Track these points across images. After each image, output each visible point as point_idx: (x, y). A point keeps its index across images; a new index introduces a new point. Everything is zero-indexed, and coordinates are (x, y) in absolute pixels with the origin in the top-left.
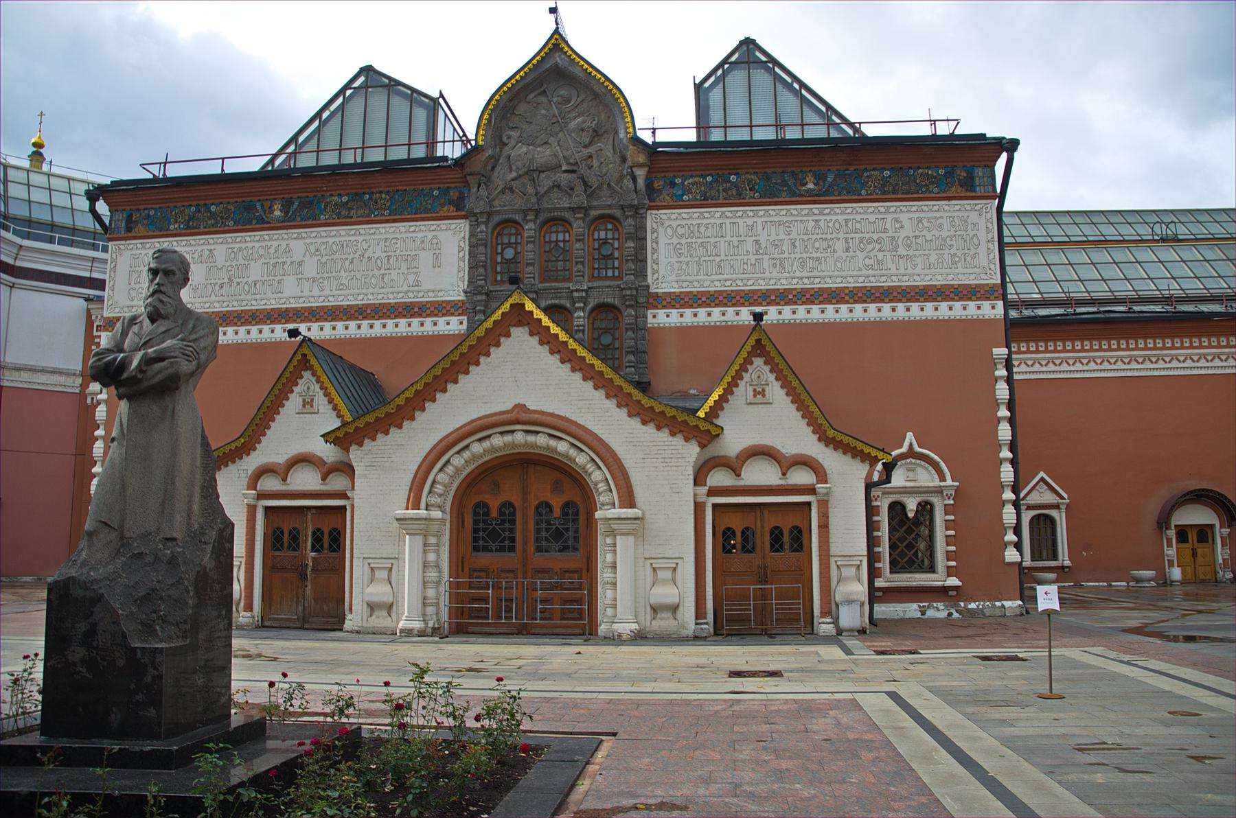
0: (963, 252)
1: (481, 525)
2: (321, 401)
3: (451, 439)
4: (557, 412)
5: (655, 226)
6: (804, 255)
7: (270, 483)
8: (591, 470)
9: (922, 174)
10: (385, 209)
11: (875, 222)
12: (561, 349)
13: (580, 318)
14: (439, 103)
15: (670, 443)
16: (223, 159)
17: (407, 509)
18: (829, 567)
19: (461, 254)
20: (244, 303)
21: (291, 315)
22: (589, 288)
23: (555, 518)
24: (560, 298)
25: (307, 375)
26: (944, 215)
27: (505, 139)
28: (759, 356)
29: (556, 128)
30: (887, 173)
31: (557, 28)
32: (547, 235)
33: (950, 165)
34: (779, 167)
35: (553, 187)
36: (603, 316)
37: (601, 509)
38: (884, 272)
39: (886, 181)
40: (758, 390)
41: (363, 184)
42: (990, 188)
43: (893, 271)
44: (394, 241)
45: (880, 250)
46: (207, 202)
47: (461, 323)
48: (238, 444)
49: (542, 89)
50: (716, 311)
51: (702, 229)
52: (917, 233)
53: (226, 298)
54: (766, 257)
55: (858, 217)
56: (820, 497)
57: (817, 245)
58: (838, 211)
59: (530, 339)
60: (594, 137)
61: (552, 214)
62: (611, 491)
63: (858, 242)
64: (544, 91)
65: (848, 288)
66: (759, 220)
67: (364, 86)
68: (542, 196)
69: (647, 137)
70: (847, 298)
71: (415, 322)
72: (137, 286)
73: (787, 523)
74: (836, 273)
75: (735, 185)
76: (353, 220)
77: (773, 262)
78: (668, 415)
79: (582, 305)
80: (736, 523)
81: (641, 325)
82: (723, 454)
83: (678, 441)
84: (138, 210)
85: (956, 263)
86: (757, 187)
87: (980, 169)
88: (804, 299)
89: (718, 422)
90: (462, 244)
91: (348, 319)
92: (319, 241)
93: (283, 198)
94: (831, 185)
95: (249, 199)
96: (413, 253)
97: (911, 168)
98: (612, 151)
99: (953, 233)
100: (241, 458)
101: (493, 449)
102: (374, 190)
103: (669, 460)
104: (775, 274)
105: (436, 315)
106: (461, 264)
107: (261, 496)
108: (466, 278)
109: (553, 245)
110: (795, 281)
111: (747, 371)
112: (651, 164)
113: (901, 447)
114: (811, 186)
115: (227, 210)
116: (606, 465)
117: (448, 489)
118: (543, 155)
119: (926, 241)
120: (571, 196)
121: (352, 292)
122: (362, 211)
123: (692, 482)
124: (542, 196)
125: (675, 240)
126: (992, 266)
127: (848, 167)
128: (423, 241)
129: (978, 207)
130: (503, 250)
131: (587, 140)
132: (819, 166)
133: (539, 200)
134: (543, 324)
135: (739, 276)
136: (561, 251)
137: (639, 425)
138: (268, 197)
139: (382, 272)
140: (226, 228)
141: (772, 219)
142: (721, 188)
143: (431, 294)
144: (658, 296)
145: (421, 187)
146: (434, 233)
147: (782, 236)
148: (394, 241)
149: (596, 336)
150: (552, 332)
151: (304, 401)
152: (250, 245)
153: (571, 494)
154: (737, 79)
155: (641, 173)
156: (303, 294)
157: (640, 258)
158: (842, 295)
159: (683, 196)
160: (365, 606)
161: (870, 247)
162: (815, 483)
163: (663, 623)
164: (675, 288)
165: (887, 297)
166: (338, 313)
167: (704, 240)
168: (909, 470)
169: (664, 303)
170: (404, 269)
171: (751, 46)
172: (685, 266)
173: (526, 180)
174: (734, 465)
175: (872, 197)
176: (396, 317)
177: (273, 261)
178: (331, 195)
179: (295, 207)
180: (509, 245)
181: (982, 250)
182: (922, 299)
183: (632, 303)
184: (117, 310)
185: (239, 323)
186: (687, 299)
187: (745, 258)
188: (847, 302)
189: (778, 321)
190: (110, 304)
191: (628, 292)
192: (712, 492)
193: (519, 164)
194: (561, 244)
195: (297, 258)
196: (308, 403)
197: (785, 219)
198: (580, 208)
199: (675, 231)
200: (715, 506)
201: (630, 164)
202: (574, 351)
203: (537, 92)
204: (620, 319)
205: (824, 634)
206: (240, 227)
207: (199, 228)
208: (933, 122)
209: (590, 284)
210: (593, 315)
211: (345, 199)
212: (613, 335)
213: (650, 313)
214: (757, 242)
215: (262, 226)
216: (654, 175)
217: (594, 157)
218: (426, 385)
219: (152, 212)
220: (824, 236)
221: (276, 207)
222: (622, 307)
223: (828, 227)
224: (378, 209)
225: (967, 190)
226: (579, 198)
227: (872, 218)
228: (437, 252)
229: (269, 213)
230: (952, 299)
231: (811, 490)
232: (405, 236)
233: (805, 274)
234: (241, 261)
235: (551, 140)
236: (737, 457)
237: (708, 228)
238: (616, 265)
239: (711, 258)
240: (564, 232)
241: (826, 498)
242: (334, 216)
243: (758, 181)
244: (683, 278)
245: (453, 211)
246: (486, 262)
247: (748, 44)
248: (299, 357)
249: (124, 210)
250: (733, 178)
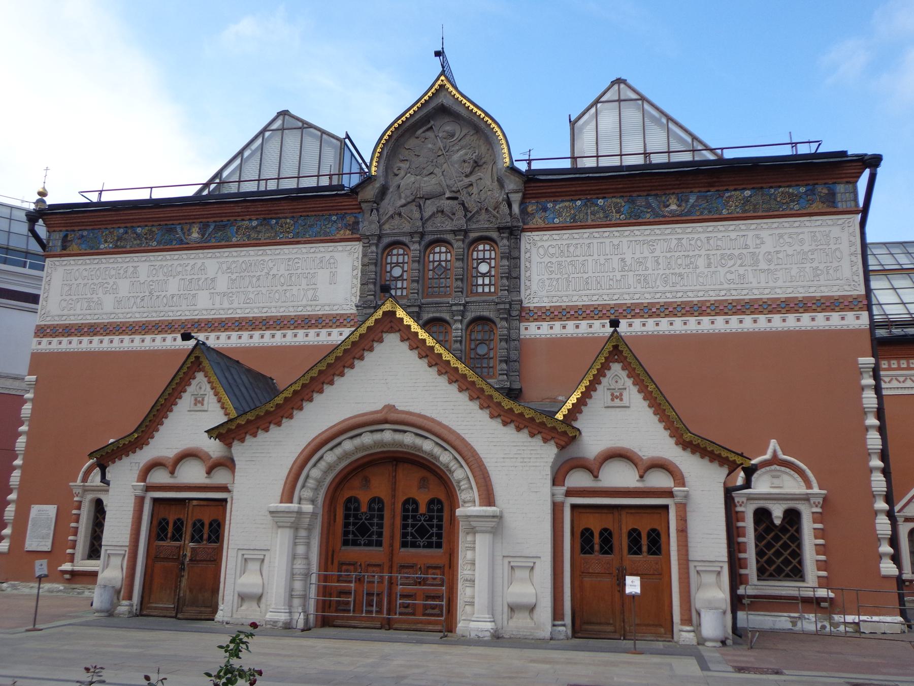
0: (826, 265)
1: (352, 520)
2: (211, 401)
3: (324, 437)
4: (423, 413)
5: (528, 246)
6: (667, 272)
7: (159, 477)
8: (454, 468)
9: (782, 193)
10: (289, 233)
11: (736, 239)
12: (428, 353)
13: (457, 328)
14: (345, 144)
15: (529, 444)
16: (151, 188)
17: (281, 502)
18: (688, 573)
19: (355, 273)
20: (162, 314)
21: (203, 325)
22: (467, 303)
23: (421, 515)
24: (440, 312)
25: (200, 376)
26: (806, 230)
27: (396, 171)
28: (617, 361)
29: (441, 160)
30: (747, 193)
31: (443, 71)
32: (431, 256)
33: (811, 182)
34: (644, 191)
35: (438, 212)
36: (480, 328)
37: (463, 506)
38: (745, 285)
39: (747, 201)
40: (615, 394)
41: (271, 210)
42: (853, 203)
43: (755, 284)
44: (296, 260)
45: (741, 265)
46: (134, 225)
48: (132, 439)
49: (429, 126)
50: (584, 324)
51: (572, 249)
52: (778, 249)
53: (146, 309)
54: (631, 274)
55: (720, 235)
56: (677, 500)
57: (679, 262)
58: (700, 229)
59: (402, 343)
60: (475, 167)
61: (436, 236)
62: (472, 488)
63: (719, 258)
64: (431, 128)
65: (709, 301)
66: (625, 240)
67: (282, 129)
68: (427, 220)
69: (523, 167)
70: (708, 311)
71: (312, 332)
72: (68, 298)
73: (644, 525)
74: (698, 287)
75: (602, 208)
76: (260, 242)
77: (638, 278)
78: (527, 416)
79: (460, 318)
80: (595, 524)
81: (514, 336)
82: (581, 455)
83: (537, 441)
84: (74, 231)
85: (818, 275)
86: (622, 209)
87: (842, 186)
88: (667, 312)
89: (576, 424)
90: (356, 264)
91: (253, 329)
92: (231, 260)
93: (201, 222)
94: (693, 206)
95: (171, 222)
96: (312, 272)
97: (771, 187)
98: (490, 180)
99: (814, 247)
101: (364, 447)
102: (280, 216)
103: (528, 460)
104: (639, 289)
105: (331, 327)
106: (355, 281)
107: (149, 488)
108: (358, 294)
109: (436, 264)
110: (658, 295)
111: (605, 376)
112: (525, 190)
113: (765, 454)
114: (673, 207)
115: (151, 232)
116: (468, 464)
117: (321, 484)
118: (429, 184)
119: (787, 255)
120: (453, 220)
121: (257, 305)
122: (269, 235)
123: (549, 482)
124: (427, 220)
125: (547, 259)
126: (856, 278)
127: (710, 189)
128: (322, 261)
129: (840, 222)
130: (392, 268)
131: (468, 170)
132: (681, 188)
133: (423, 224)
134: (412, 330)
135: (605, 291)
136: (443, 269)
137: (500, 426)
138: (188, 221)
139: (285, 287)
140: (150, 248)
141: (637, 238)
142: (589, 211)
143: (327, 308)
144: (530, 310)
145: (321, 213)
146: (332, 254)
147: (646, 254)
148: (296, 260)
149: (473, 346)
150: (420, 337)
151: (196, 400)
152: (169, 263)
155: (516, 198)
156: (215, 307)
157: (514, 275)
158: (704, 308)
159: (555, 218)
160: (236, 596)
161: (731, 263)
162: (673, 486)
163: (520, 624)
164: (546, 303)
165: (748, 309)
166: (244, 324)
167: (573, 258)
168: (773, 477)
169: (536, 317)
170: (304, 286)
171: (622, 86)
172: (555, 283)
173: (413, 207)
174: (592, 468)
175: (733, 216)
176: (295, 328)
177: (189, 277)
178: (243, 220)
179: (211, 230)
180: (397, 264)
181: (846, 265)
182: (784, 311)
183: (506, 316)
184: (48, 319)
185: (156, 332)
186: (556, 313)
187: (611, 275)
188: (709, 315)
189: (642, 332)
190: (43, 313)
191: (502, 306)
192: (570, 493)
193: (408, 192)
194: (443, 264)
195: (211, 274)
196: (199, 402)
197: (649, 238)
198: (460, 230)
199: (546, 251)
200: (574, 507)
201: (507, 191)
202: (440, 355)
203: (424, 128)
204: (495, 331)
205: (683, 643)
206: (162, 247)
207: (125, 247)
208: (794, 145)
209: (468, 299)
210: (471, 327)
211: (254, 223)
212: (488, 346)
213: (523, 325)
214: (623, 260)
215: (181, 246)
216: (528, 201)
217: (475, 185)
218: (304, 386)
219: (85, 233)
220: (686, 253)
221: (194, 230)
222: (497, 320)
223: (690, 244)
224: (282, 232)
225: (828, 206)
226: (460, 222)
227: (733, 235)
228: (333, 270)
229: (188, 235)
230: (815, 311)
231: (669, 494)
232: (305, 256)
233: (668, 288)
234: (161, 277)
235: (437, 171)
236: (594, 459)
237: (577, 248)
238: (493, 282)
239: (579, 275)
240: (446, 252)
241: (684, 501)
242: (245, 238)
243: (623, 204)
244: (553, 293)
245: (348, 235)
246: (376, 279)
248: (192, 359)
249: (61, 231)
250: (600, 202)
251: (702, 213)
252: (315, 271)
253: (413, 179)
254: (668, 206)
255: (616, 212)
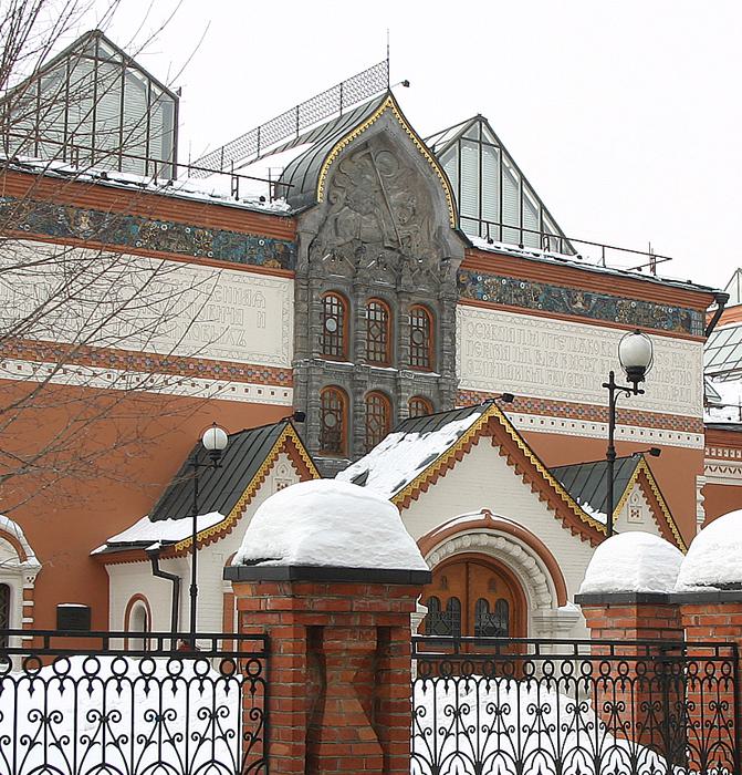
30: (634, 304)
47: (286, 395)
90: (286, 306)
94: (594, 308)
105: (262, 383)
114: (580, 305)
118: (369, 227)
153: (502, 591)
154: (469, 153)
211: (164, 227)
217: (413, 237)
229: (75, 225)
247: (480, 119)
251: (601, 317)
252: (242, 307)
253: (352, 215)
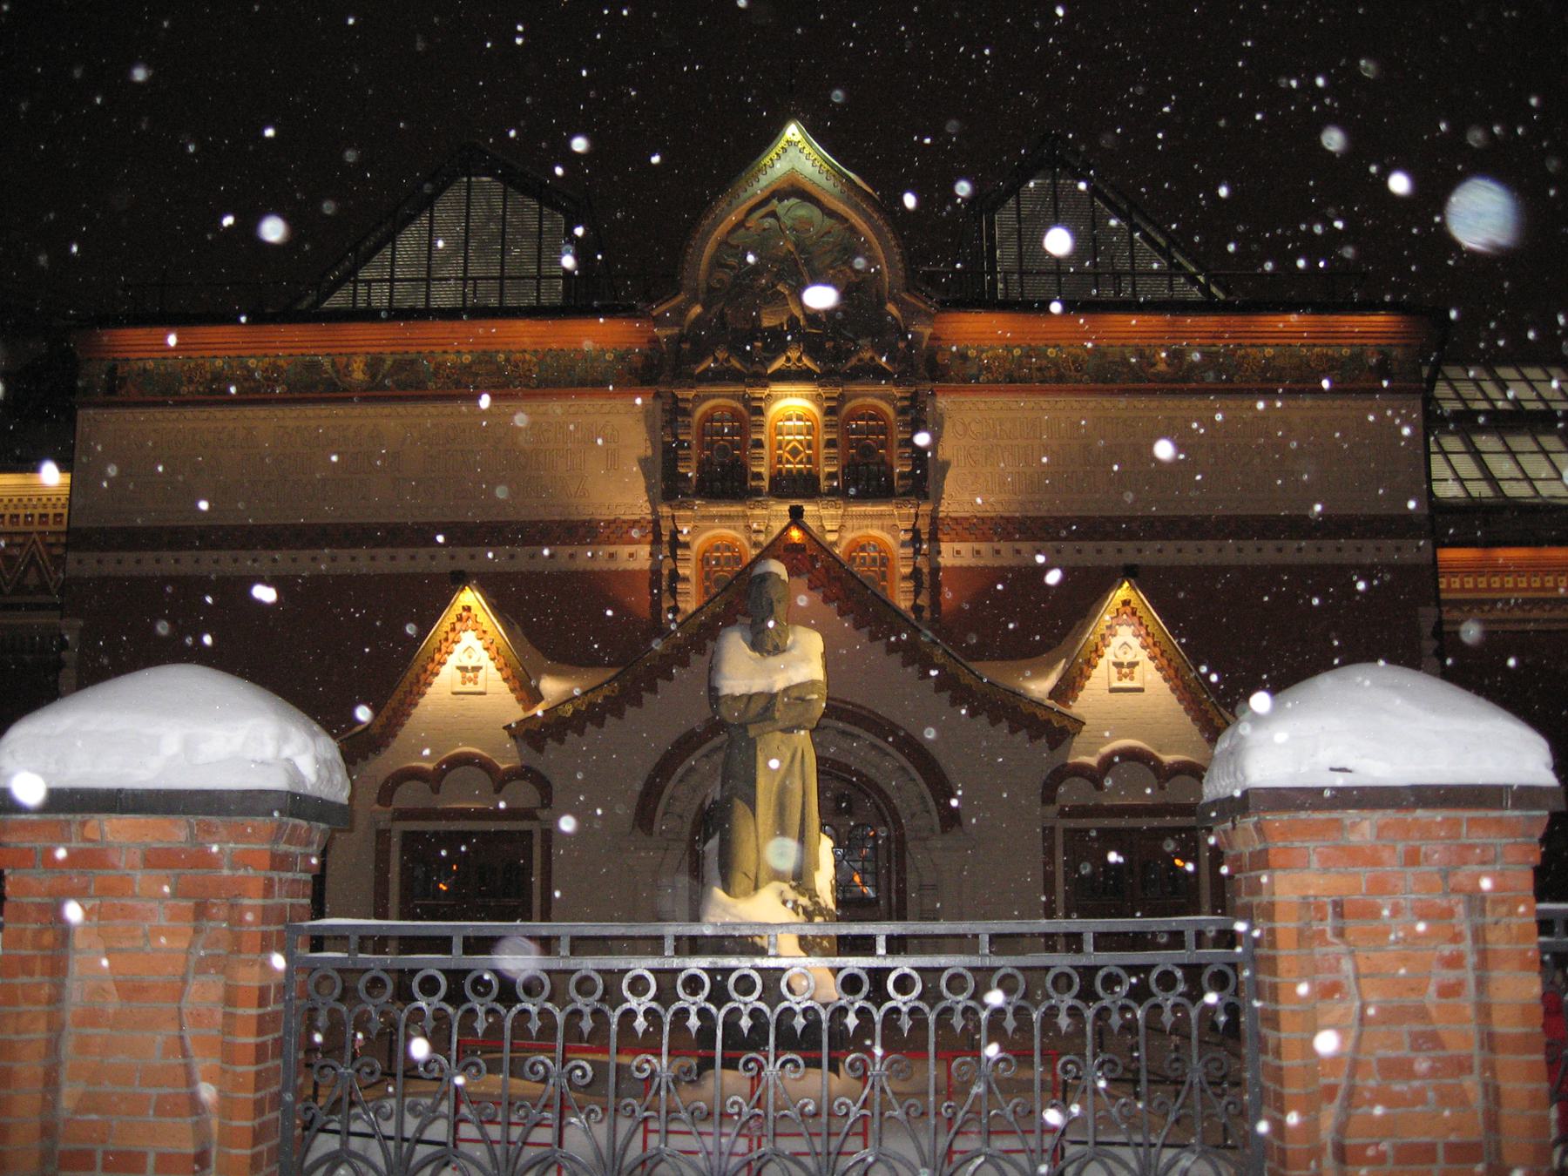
7: (409, 796)
100: (366, 758)
138: (343, 350)
178: (445, 352)
192: (1062, 814)
200: (1066, 831)
206: (297, 395)
221: (355, 366)
224: (520, 376)
254: (1154, 365)
255: (1076, 370)
